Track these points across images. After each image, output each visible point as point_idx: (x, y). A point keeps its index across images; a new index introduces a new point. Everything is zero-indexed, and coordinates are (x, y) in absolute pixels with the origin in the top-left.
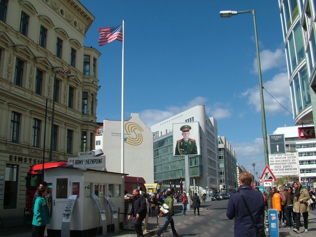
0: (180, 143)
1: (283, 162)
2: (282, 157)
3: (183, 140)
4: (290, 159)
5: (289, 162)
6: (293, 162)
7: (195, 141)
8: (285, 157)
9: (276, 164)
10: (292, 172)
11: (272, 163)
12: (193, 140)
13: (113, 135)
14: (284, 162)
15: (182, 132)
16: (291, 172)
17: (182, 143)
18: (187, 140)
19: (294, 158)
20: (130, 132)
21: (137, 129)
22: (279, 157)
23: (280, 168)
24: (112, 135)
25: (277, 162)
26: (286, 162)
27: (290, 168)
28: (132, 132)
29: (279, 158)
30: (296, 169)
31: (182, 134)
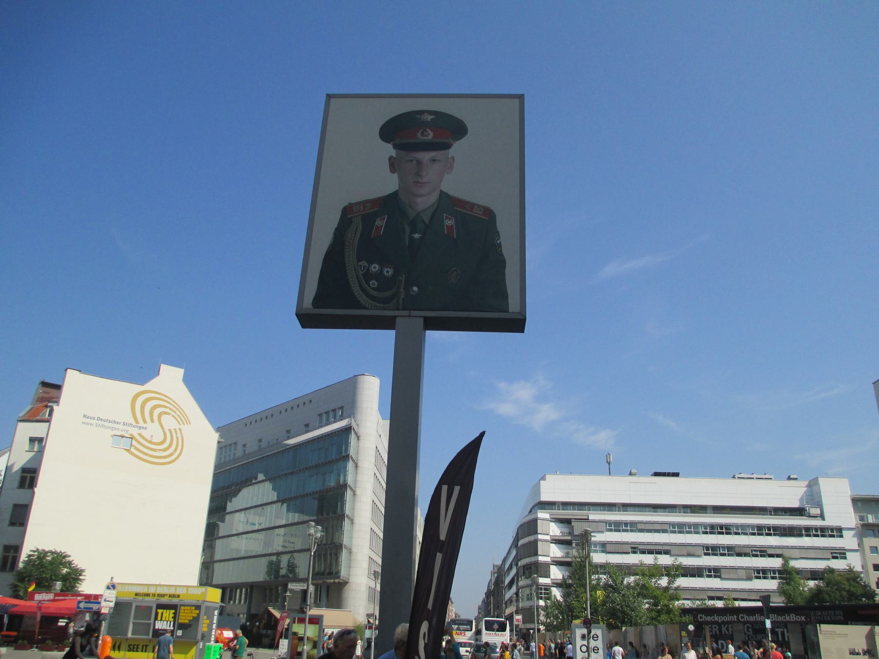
0: (368, 220)
3: (390, 204)
7: (489, 214)
12: (473, 206)
13: (88, 424)
15: (389, 150)
17: (380, 223)
18: (425, 201)
20: (145, 422)
21: (168, 414)
24: (83, 423)
28: (152, 421)
31: (393, 165)
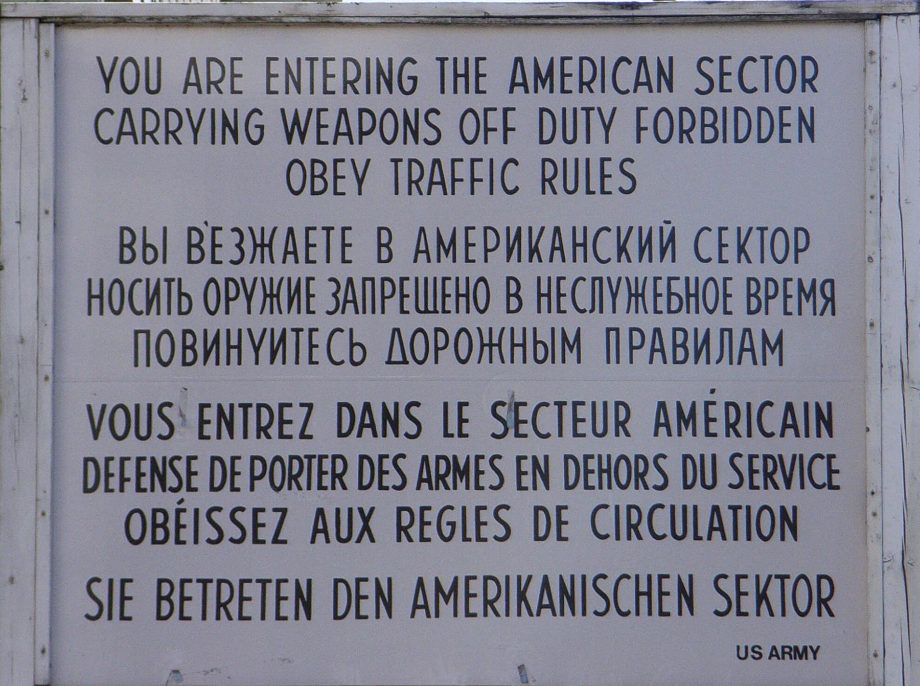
10: (686, 596)
16: (649, 593)
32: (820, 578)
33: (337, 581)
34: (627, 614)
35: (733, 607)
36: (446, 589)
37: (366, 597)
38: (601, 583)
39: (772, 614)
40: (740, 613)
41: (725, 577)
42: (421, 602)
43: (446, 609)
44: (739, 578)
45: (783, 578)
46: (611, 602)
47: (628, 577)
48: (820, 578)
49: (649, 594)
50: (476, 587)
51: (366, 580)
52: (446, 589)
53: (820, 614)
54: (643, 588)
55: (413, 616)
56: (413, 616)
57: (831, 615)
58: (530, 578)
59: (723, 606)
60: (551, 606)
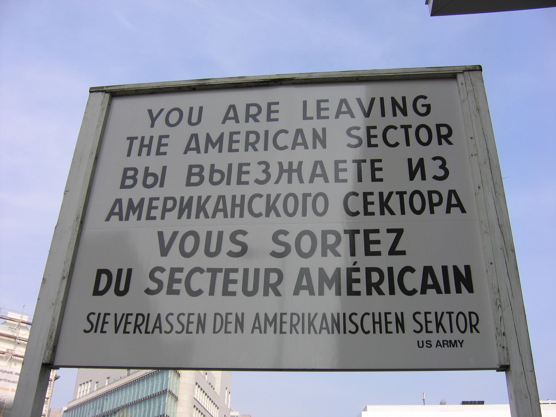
1: (283, 188)
2: (273, 128)
4: (381, 152)
5: (367, 185)
6: (418, 184)
8: (308, 128)
9: (184, 207)
10: (400, 323)
11: (138, 193)
14: (298, 189)
19: (434, 149)
22: (243, 127)
23: (223, 261)
25: (205, 190)
26: (319, 185)
27: (373, 261)
29: (242, 137)
30: (464, 280)
32: (470, 313)
33: (216, 314)
34: (369, 332)
35: (423, 328)
36: (271, 318)
37: (231, 323)
38: (353, 317)
39: (445, 332)
40: (427, 332)
41: (419, 313)
42: (257, 325)
43: (270, 329)
44: (426, 313)
45: (450, 313)
46: (359, 328)
47: (368, 314)
48: (470, 313)
49: (380, 322)
50: (287, 318)
51: (231, 314)
52: (271, 318)
53: (472, 332)
54: (377, 319)
55: (252, 332)
56: (252, 332)
57: (478, 332)
58: (316, 314)
59: (418, 328)
60: (327, 328)
